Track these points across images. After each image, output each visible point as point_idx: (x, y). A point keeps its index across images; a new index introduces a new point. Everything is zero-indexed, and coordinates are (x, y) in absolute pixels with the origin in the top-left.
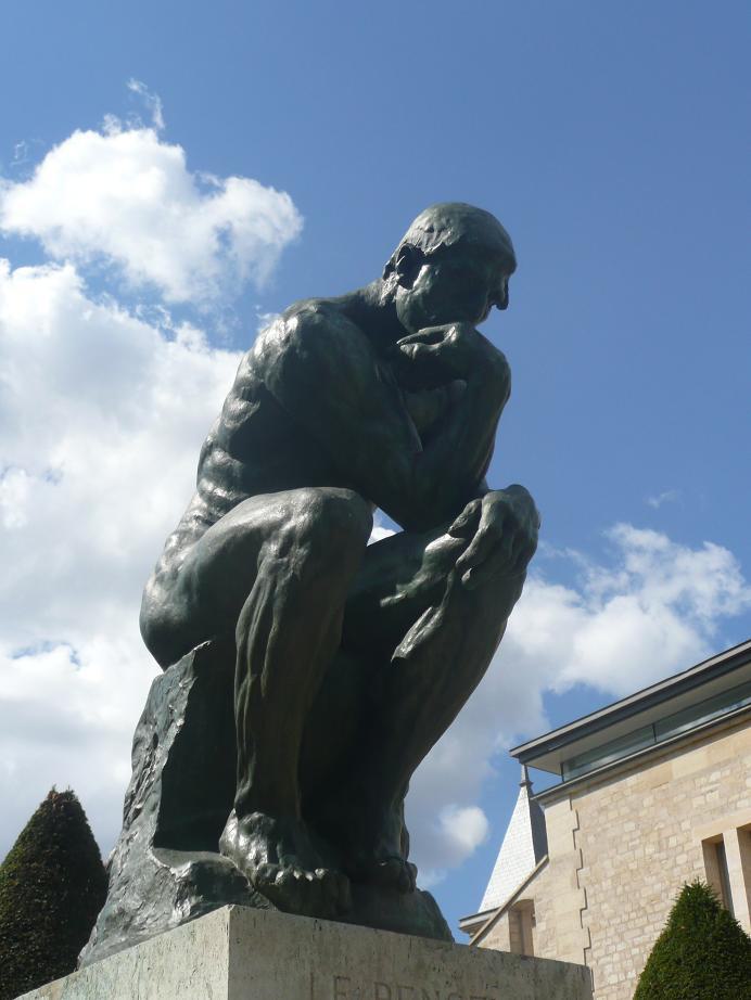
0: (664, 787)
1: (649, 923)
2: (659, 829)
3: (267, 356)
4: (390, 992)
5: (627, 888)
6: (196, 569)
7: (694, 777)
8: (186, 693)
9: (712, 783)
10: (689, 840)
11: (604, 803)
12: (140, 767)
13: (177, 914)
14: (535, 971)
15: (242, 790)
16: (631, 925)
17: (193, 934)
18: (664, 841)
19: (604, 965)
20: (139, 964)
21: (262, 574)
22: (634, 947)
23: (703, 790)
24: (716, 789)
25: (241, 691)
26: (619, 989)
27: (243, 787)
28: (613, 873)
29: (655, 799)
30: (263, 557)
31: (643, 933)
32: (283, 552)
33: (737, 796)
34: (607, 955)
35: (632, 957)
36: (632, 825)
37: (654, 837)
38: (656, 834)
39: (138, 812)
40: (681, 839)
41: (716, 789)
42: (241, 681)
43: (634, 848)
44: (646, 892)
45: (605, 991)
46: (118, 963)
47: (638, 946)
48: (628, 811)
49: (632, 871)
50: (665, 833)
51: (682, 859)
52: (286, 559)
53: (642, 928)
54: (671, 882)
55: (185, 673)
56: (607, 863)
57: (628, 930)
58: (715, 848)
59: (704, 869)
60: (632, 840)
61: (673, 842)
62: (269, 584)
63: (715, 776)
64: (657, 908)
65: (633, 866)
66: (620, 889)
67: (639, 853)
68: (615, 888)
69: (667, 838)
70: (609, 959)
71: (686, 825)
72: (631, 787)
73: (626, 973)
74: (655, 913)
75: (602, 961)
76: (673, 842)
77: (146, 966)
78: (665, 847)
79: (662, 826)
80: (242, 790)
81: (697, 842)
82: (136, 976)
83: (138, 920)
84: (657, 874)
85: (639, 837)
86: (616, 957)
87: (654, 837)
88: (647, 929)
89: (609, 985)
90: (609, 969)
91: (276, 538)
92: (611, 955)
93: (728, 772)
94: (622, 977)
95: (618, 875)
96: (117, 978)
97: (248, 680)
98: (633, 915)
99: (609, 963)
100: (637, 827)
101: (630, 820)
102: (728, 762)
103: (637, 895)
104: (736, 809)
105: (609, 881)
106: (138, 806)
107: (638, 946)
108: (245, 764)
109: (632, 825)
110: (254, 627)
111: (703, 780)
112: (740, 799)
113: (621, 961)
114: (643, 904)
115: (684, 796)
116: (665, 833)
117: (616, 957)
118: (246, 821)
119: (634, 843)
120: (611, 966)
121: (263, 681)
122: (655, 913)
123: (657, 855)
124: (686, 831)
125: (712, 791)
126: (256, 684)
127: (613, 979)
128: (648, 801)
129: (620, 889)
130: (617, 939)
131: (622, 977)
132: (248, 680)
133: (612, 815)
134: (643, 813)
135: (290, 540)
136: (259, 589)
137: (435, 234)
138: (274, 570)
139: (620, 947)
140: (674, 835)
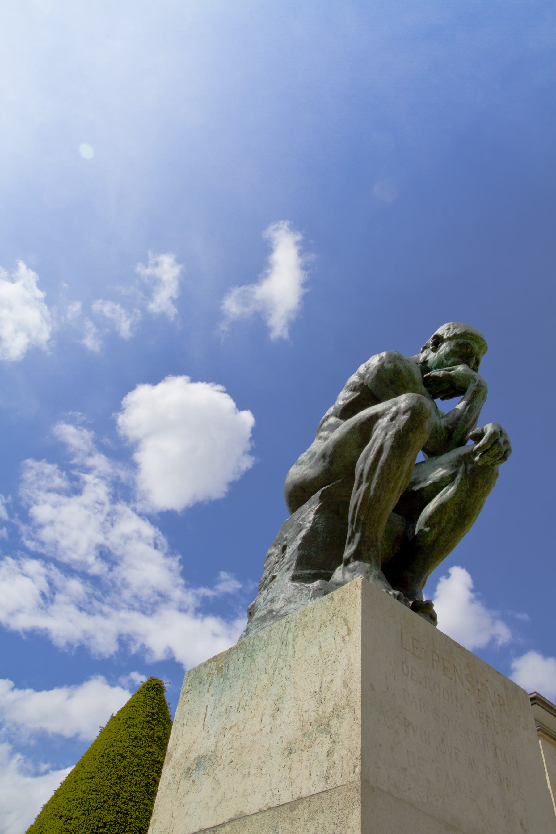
4: (438, 659)
15: (349, 551)
17: (332, 599)
20: (287, 626)
25: (357, 494)
27: (350, 549)
42: (358, 488)
46: (271, 630)
52: (394, 422)
77: (293, 625)
80: (349, 551)
82: (285, 632)
96: (269, 637)
106: (275, 574)
108: (352, 537)
121: (373, 486)
126: (368, 488)
132: (363, 487)
137: (451, 330)
138: (386, 429)
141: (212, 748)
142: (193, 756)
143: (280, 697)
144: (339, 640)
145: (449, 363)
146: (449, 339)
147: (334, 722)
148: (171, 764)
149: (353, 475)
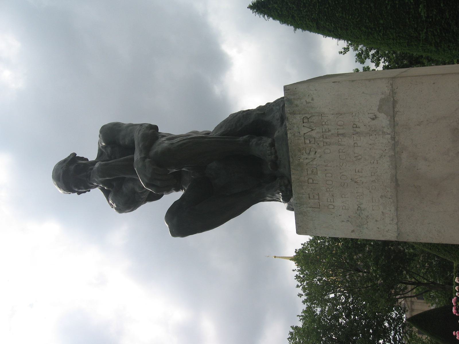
14: (290, 113)
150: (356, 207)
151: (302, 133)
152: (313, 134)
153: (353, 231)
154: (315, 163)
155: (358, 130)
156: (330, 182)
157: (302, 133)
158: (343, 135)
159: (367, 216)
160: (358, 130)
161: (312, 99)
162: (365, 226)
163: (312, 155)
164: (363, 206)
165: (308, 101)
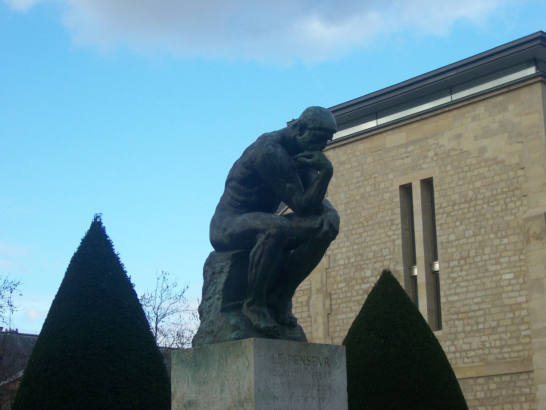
0: (380, 152)
1: (365, 231)
2: (375, 177)
3: (255, 159)
5: (353, 210)
6: (236, 232)
7: (398, 147)
8: (229, 266)
9: (408, 152)
10: (392, 185)
11: (344, 158)
12: (208, 279)
13: (233, 335)
15: (248, 300)
16: (354, 232)
18: (377, 185)
19: (337, 254)
21: (258, 243)
22: (355, 244)
23: (403, 156)
24: (410, 156)
26: (344, 268)
28: (345, 201)
29: (374, 159)
30: (259, 237)
31: (361, 237)
32: (266, 238)
33: (422, 162)
34: (338, 248)
35: (353, 250)
36: (359, 174)
37: (371, 181)
38: (373, 180)
39: (210, 298)
40: (388, 184)
41: (410, 156)
43: (358, 188)
44: (365, 213)
45: (336, 268)
47: (358, 244)
48: (357, 165)
49: (357, 200)
50: (378, 180)
51: (387, 196)
53: (360, 234)
54: (379, 209)
55: (228, 259)
56: (342, 195)
57: (352, 234)
58: (406, 189)
59: (399, 203)
60: (358, 182)
61: (382, 185)
62: (262, 247)
63: (410, 148)
64: (370, 223)
65: (358, 198)
66: (349, 211)
67: (362, 190)
68: (346, 210)
69: (379, 183)
70: (340, 250)
71: (391, 176)
72: (360, 150)
73: (349, 260)
74: (369, 226)
75: (335, 252)
76: (382, 185)
78: (377, 188)
79: (377, 175)
81: (398, 187)
83: (219, 335)
84: (371, 204)
85: (363, 181)
86: (344, 250)
87: (371, 181)
88: (363, 235)
89: (339, 265)
90: (339, 256)
91: (265, 233)
92: (341, 248)
93: (418, 147)
94: (347, 261)
95: (348, 203)
97: (254, 271)
98: (356, 226)
99: (340, 253)
100: (362, 175)
101: (358, 171)
102: (419, 140)
103: (359, 215)
104: (421, 169)
105: (343, 206)
107: (358, 244)
109: (359, 174)
110: (257, 257)
111: (403, 150)
112: (424, 163)
113: (347, 252)
114: (362, 220)
115: (390, 159)
116: (378, 180)
117: (344, 250)
118: (251, 308)
119: (358, 184)
120: (341, 254)
122: (369, 226)
123: (372, 193)
124: (391, 180)
125: (407, 157)
127: (342, 262)
128: (370, 160)
129: (349, 211)
130: (345, 239)
131: (347, 261)
132: (254, 271)
133: (347, 166)
134: (365, 167)
135: (269, 235)
136: (259, 247)
138: (263, 243)
139: (347, 244)
140: (384, 181)
141: (195, 399)
142: (186, 400)
143: (222, 385)
144: (245, 368)
145: (310, 147)
146: (310, 129)
147: (245, 404)
148: (175, 400)
149: (248, 260)
150: (276, 395)
151: (319, 355)
152: (319, 365)
153: (259, 390)
154: (302, 363)
155: (321, 402)
156: (290, 375)
157: (319, 355)
158: (318, 390)
159: (270, 404)
160: (321, 402)
161: (338, 368)
162: (263, 401)
163: (306, 362)
164: (276, 400)
165: (337, 364)
